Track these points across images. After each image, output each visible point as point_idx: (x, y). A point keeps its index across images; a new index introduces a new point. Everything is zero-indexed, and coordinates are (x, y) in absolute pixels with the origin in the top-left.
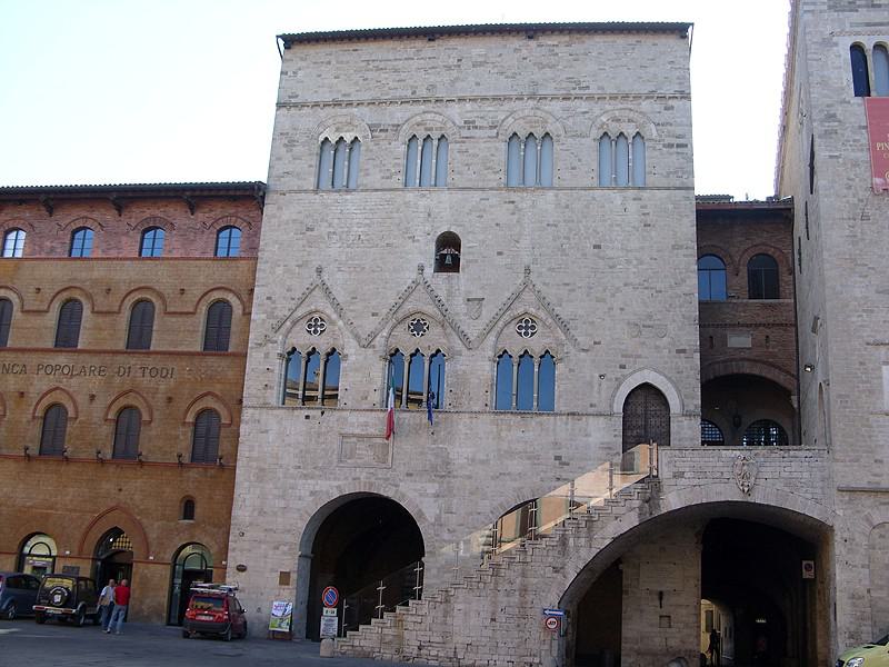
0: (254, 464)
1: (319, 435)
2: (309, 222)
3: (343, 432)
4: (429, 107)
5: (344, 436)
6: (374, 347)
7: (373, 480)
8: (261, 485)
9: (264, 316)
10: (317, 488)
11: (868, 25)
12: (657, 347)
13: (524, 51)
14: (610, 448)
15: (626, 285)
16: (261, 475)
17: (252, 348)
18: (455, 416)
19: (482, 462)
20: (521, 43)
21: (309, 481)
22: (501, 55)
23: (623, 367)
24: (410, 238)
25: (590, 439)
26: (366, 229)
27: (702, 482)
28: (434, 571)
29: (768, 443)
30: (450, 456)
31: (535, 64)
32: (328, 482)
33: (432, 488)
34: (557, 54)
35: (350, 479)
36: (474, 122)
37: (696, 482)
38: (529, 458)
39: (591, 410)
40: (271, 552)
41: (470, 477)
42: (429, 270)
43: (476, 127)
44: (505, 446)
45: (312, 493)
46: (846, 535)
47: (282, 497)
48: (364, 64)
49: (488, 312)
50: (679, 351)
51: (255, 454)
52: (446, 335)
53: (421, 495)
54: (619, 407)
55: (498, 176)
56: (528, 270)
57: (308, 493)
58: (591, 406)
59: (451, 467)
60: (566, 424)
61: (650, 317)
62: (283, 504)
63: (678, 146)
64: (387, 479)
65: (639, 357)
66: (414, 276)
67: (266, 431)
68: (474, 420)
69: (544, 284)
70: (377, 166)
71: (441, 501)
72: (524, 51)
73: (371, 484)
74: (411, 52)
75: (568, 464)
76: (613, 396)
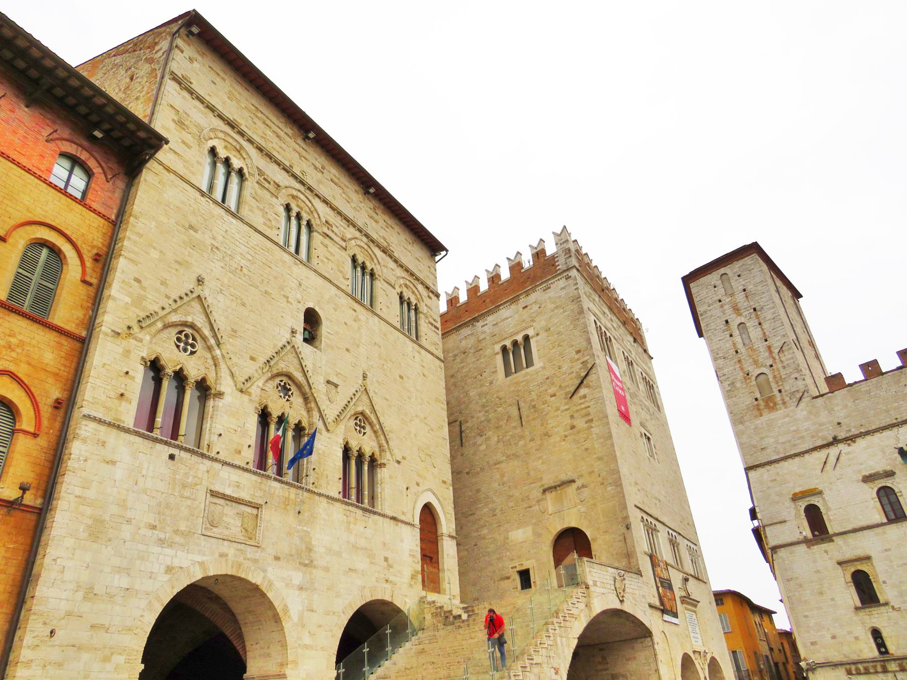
0: (89, 511)
1: (184, 486)
2: (193, 220)
4: (308, 193)
5: (214, 494)
6: (250, 394)
10: (176, 563)
15: (417, 416)
16: (97, 531)
18: (317, 497)
21: (168, 551)
26: (248, 264)
32: (190, 556)
33: (298, 577)
35: (217, 555)
39: (402, 518)
41: (327, 569)
44: (352, 539)
45: (169, 570)
51: (91, 494)
52: (309, 411)
54: (417, 521)
56: (365, 377)
58: (403, 513)
62: (124, 582)
64: (255, 561)
66: (288, 336)
67: (113, 463)
68: (331, 506)
71: (304, 594)
73: (240, 565)
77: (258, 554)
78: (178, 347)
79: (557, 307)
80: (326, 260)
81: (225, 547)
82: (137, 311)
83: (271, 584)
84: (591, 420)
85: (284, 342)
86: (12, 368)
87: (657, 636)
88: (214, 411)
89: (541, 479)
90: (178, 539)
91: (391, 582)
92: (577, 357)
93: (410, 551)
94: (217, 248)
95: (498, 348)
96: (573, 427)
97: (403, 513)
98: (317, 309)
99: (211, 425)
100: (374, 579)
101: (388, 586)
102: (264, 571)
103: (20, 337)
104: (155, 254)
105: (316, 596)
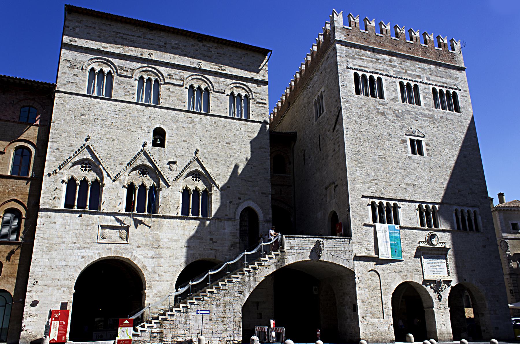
0: (46, 241)
2: (82, 111)
3: (102, 224)
7: (118, 249)
8: (50, 253)
9: (54, 159)
10: (86, 254)
11: (360, 66)
12: (254, 191)
13: (197, 47)
14: (234, 235)
16: (50, 247)
17: (46, 176)
19: (175, 241)
20: (195, 42)
21: (81, 251)
22: (185, 46)
23: (239, 199)
24: (139, 127)
25: (226, 231)
27: (302, 251)
28: (151, 297)
29: (341, 235)
30: (160, 238)
31: (201, 54)
32: (92, 251)
33: (151, 253)
34: (211, 52)
35: (106, 249)
36: (172, 76)
37: (299, 251)
38: (198, 239)
40: (55, 291)
42: (150, 144)
43: (173, 79)
45: (83, 257)
46: (359, 275)
47: (65, 260)
48: (114, 34)
49: (177, 169)
50: (263, 193)
51: (47, 235)
53: (144, 257)
54: (238, 217)
55: (184, 104)
57: (80, 257)
59: (160, 243)
60: (215, 223)
61: (251, 177)
62: (64, 264)
63: (263, 103)
65: (246, 194)
67: (55, 223)
69: (205, 158)
70: (122, 88)
71: (155, 260)
72: (197, 47)
73: (118, 252)
74: (140, 34)
75: (216, 242)
76: (235, 212)
77: (128, 246)
78: (82, 170)
80: (168, 98)
81: (109, 246)
82: (59, 162)
83: (135, 258)
85: (139, 151)
86: (15, 198)
90: (86, 246)
91: (215, 250)
93: (231, 233)
94: (97, 119)
97: (226, 215)
98: (162, 126)
100: (201, 249)
101: (213, 252)
102: (132, 253)
103: (17, 186)
104: (64, 135)
105: (162, 260)
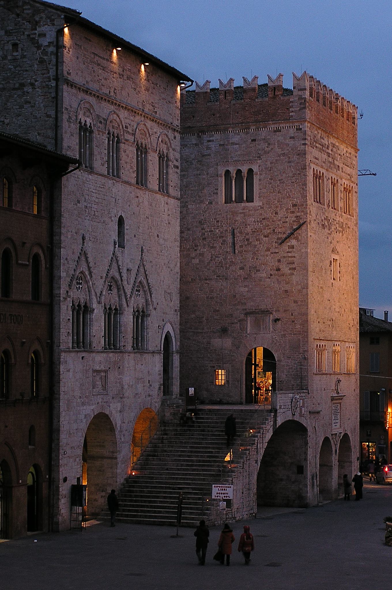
79: (284, 154)
84: (295, 269)
87: (309, 429)
88: (90, 321)
89: (245, 304)
92: (292, 209)
95: (222, 171)
96: (278, 270)
99: (90, 331)
